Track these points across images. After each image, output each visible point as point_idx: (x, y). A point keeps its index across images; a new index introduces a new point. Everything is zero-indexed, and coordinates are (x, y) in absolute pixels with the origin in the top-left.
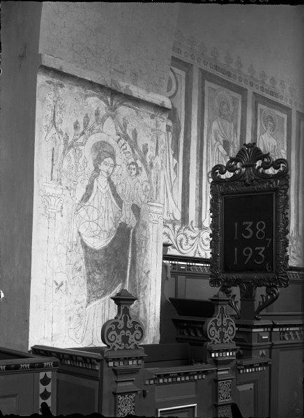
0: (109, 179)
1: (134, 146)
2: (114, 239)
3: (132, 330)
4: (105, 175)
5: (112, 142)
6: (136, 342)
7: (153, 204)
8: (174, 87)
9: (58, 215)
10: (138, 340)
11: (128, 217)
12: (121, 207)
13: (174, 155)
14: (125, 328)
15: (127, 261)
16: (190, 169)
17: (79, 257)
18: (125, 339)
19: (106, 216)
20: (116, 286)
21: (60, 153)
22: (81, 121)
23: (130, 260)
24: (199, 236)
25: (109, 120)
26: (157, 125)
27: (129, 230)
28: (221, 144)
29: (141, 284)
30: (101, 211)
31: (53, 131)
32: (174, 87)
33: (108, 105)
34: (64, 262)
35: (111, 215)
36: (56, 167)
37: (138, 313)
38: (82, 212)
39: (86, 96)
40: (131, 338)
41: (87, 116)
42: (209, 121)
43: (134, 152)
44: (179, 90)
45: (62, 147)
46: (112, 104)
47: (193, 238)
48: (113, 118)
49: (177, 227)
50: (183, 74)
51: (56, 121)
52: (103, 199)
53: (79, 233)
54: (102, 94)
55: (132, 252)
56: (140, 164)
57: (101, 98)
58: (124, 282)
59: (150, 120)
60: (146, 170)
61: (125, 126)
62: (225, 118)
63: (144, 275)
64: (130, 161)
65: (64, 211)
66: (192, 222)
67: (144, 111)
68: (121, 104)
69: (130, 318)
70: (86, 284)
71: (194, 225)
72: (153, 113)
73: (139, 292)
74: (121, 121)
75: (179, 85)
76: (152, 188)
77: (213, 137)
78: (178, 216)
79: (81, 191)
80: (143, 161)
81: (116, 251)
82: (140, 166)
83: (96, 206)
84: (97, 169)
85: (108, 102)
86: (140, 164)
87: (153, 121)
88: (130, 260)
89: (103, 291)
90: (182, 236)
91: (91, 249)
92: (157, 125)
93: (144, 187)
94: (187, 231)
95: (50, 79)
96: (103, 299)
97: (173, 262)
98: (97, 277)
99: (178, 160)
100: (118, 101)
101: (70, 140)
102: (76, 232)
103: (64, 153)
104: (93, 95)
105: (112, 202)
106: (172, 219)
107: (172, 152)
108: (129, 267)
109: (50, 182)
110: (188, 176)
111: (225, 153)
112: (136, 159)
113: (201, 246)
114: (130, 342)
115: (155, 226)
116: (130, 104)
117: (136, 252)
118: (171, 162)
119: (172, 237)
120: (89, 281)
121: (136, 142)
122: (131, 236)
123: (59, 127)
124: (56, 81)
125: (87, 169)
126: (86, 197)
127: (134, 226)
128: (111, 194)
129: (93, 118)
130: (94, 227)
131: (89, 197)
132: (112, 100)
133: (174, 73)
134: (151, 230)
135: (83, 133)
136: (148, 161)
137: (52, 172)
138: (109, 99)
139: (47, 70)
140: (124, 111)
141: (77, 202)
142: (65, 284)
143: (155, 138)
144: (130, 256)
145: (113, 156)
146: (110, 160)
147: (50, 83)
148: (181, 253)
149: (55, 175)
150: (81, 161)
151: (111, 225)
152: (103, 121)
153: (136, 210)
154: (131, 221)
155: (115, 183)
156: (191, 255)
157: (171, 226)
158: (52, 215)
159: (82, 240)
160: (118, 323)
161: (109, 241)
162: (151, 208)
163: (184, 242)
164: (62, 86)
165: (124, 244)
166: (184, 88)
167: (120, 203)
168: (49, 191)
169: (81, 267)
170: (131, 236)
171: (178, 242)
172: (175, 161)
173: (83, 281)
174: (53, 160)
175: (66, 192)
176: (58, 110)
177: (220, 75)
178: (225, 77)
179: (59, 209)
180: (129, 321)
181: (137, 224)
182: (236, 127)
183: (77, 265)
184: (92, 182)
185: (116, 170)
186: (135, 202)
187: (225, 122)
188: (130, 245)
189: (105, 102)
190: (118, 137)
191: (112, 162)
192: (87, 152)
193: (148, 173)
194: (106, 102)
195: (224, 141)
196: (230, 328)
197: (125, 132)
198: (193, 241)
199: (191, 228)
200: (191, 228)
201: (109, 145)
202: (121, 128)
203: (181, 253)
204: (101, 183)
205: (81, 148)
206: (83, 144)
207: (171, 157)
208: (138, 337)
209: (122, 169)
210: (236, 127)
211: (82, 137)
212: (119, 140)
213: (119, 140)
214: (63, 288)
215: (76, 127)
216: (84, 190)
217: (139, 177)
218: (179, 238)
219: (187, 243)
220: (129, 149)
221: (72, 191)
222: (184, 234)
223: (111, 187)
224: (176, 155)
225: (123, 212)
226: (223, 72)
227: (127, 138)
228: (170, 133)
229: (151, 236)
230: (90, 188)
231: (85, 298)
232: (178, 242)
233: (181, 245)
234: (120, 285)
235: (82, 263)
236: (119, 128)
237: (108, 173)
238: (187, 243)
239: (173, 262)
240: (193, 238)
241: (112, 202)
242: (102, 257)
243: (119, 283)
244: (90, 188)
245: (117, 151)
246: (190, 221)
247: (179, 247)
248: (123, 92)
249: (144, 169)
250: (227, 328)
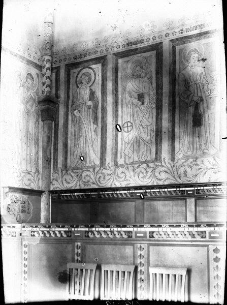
16: (108, 127)
28: (135, 98)
32: (93, 78)
49: (97, 169)
71: (110, 165)
78: (98, 162)
90: (100, 175)
97: (181, 189)
111: (140, 103)
113: (116, 179)
119: (92, 177)
157: (91, 170)
163: (102, 179)
166: (100, 75)
171: (97, 179)
172: (95, 126)
195: (139, 95)
198: (110, 177)
199: (108, 168)
200: (108, 168)
207: (92, 123)
218: (98, 176)
222: (101, 173)
233: (99, 181)
239: (181, 189)
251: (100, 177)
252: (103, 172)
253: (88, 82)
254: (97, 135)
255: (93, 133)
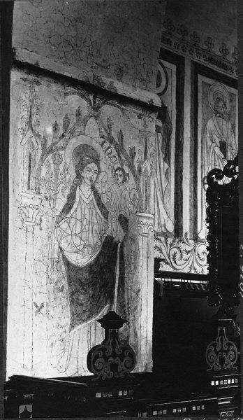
0: (93, 188)
1: (120, 150)
2: (99, 255)
3: (122, 357)
4: (88, 182)
5: (96, 145)
6: (126, 370)
7: (143, 214)
8: (164, 82)
9: (37, 228)
10: (128, 368)
11: (115, 230)
12: (107, 219)
13: (164, 159)
14: (114, 355)
15: (115, 279)
16: (183, 174)
17: (60, 275)
18: (114, 367)
19: (91, 229)
20: (103, 307)
21: (38, 160)
22: (61, 122)
23: (117, 277)
24: (194, 249)
25: (92, 120)
26: (145, 125)
27: (116, 244)
29: (130, 305)
30: (85, 223)
31: (30, 134)
32: (164, 82)
33: (91, 104)
34: (44, 281)
35: (96, 227)
36: (34, 174)
37: (128, 338)
38: (64, 225)
39: (66, 94)
40: (122, 366)
41: (67, 117)
42: (203, 119)
43: (120, 157)
44: (169, 86)
45: (39, 153)
46: (95, 102)
47: (188, 252)
48: (96, 119)
49: (170, 240)
50: (174, 68)
51: (33, 122)
52: (87, 211)
53: (60, 248)
54: (83, 92)
55: (120, 269)
56: (126, 168)
57: (83, 96)
58: (112, 302)
59: (138, 120)
60: (134, 176)
61: (110, 127)
62: (221, 116)
63: (134, 294)
64: (116, 167)
65: (43, 224)
66: (186, 234)
67: (130, 110)
68: (104, 103)
69: (119, 344)
70: (69, 308)
72: (140, 112)
73: (129, 314)
74: (105, 122)
75: (170, 81)
76: (140, 196)
77: (208, 139)
78: (171, 228)
79: (61, 202)
80: (131, 166)
81: (101, 268)
82: (127, 171)
83: (79, 218)
84: (79, 176)
85: (90, 100)
86: (126, 168)
87: (141, 121)
88: (117, 277)
89: (88, 313)
90: (175, 250)
91: (75, 267)
92: (145, 125)
93: (132, 197)
94: (181, 244)
95: (26, 76)
96: (89, 322)
97: (166, 280)
98: (82, 297)
99: (169, 165)
100: (101, 99)
101: (49, 143)
102: (57, 247)
103: (42, 158)
104: (74, 93)
105: (96, 213)
106: (164, 231)
107: (162, 156)
108: (117, 285)
109: (28, 191)
110: (181, 183)
111: (222, 156)
112: (122, 165)
113: (196, 261)
114: (119, 371)
115: (146, 240)
116: (115, 103)
117: (125, 268)
118: (162, 166)
119: (164, 251)
120: (72, 302)
121: (122, 145)
122: (119, 251)
123: (36, 129)
124: (31, 77)
125: (68, 177)
126: (68, 208)
127: (121, 239)
128: (95, 204)
129: (73, 119)
130: (78, 241)
131: (70, 208)
132: (94, 97)
133: (164, 67)
134: (140, 244)
135: (63, 136)
136: (136, 166)
137: (29, 180)
138: (91, 97)
139: (22, 66)
140: (108, 110)
141: (58, 213)
142: (45, 306)
143: (143, 140)
144: (118, 273)
145: (97, 161)
146: (93, 166)
147: (25, 80)
148: (175, 268)
149: (33, 184)
150: (61, 167)
151: (96, 239)
152: (85, 122)
153: (124, 221)
154: (119, 235)
155: (100, 192)
156: (186, 271)
157: (163, 239)
158: (30, 229)
159: (64, 257)
160: (106, 349)
161: (93, 258)
162: (141, 219)
163: (178, 257)
164: (38, 83)
165: (112, 260)
166: (175, 83)
167: (106, 214)
168: (26, 201)
169: (63, 287)
170: (119, 251)
171: (171, 257)
173: (65, 302)
174: (30, 166)
175: (46, 203)
176: (34, 110)
177: (215, 68)
178: (221, 71)
179: (37, 222)
180: (118, 346)
181: (125, 237)
182: (233, 127)
183: (59, 284)
184: (75, 190)
185: (100, 177)
186: (122, 213)
187: (222, 122)
188: (118, 261)
189: (86, 100)
190: (103, 140)
191: (96, 168)
192: (67, 157)
193: (137, 179)
194: (89, 101)
196: (231, 352)
197: (109, 134)
198: (189, 255)
201: (93, 149)
202: (106, 130)
203: (175, 268)
204: (84, 192)
205: (62, 152)
206: (63, 149)
207: (162, 161)
208: (129, 364)
209: (106, 176)
210: (233, 127)
211: (62, 141)
212: (103, 143)
213: (103, 143)
214: (44, 310)
215: (55, 129)
216: (65, 200)
217: (126, 185)
218: (172, 253)
219: (181, 257)
220: (114, 153)
221: (52, 202)
222: (177, 248)
223: (95, 197)
224: (167, 159)
225: (110, 224)
226: (219, 64)
227: (112, 141)
228: (160, 134)
229: (141, 250)
230: (72, 197)
231: (68, 321)
232: (171, 257)
233: (174, 259)
234: (107, 305)
235: (64, 282)
236: (103, 130)
237: (91, 180)
238: (181, 257)
239: (166, 280)
240: (188, 252)
241: (96, 213)
242: (86, 275)
243: (106, 304)
244: (72, 197)
245: (102, 154)
246: (184, 233)
247: (173, 262)
248: (107, 89)
249: (132, 177)
250: (227, 352)
251: (175, 254)
252: (179, 246)
253: (158, 85)
254: (169, 183)
255: (163, 176)
